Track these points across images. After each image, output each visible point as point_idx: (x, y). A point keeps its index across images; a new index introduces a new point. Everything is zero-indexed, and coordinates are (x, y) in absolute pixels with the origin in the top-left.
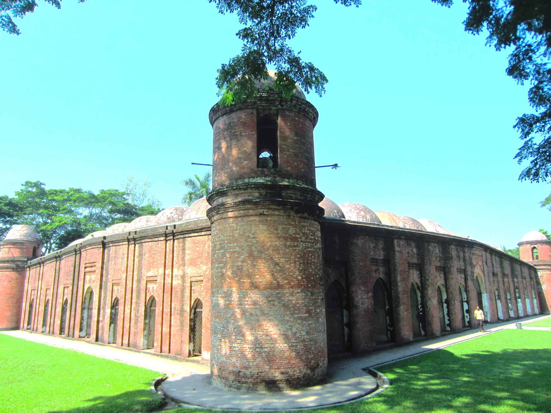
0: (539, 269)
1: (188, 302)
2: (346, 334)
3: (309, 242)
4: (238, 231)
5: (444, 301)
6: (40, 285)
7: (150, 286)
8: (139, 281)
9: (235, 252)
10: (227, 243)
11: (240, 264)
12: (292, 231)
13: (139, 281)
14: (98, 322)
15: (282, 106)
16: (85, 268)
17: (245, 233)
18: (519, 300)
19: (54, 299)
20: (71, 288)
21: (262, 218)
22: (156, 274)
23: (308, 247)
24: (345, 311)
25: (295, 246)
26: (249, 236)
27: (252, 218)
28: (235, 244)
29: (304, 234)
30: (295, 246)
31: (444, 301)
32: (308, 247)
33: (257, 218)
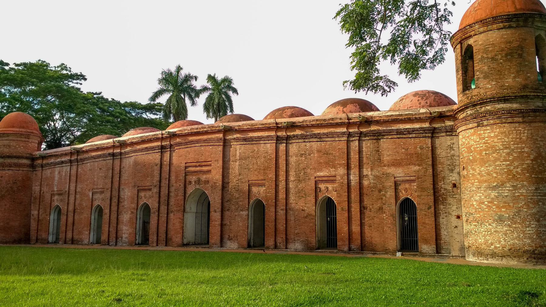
1: (393, 201)
4: (525, 135)
6: (72, 188)
7: (322, 186)
9: (523, 152)
10: (514, 144)
11: (528, 162)
14: (222, 225)
16: (186, 167)
17: (533, 136)
19: (114, 204)
20: (155, 190)
22: (333, 173)
26: (536, 139)
27: (537, 124)
28: (524, 145)
33: (542, 124)
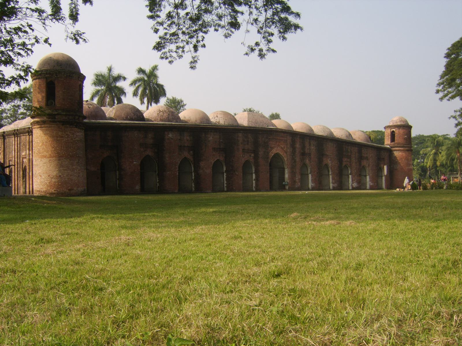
0: (395, 151)
2: (117, 184)
3: (69, 138)
5: (224, 171)
7: (24, 160)
8: (20, 158)
11: (39, 148)
12: (60, 133)
13: (20, 158)
15: (57, 76)
18: (350, 176)
21: (47, 128)
23: (69, 140)
24: (117, 172)
25: (61, 140)
27: (43, 128)
29: (67, 134)
30: (61, 140)
31: (224, 171)
32: (69, 140)
